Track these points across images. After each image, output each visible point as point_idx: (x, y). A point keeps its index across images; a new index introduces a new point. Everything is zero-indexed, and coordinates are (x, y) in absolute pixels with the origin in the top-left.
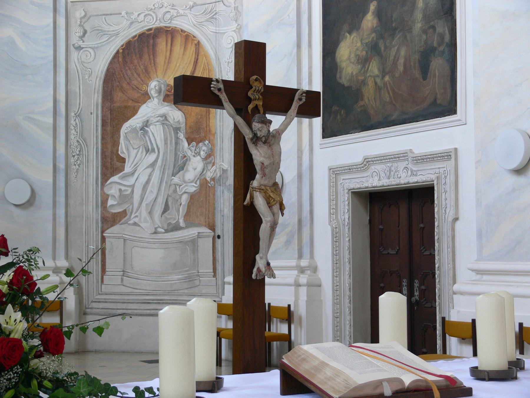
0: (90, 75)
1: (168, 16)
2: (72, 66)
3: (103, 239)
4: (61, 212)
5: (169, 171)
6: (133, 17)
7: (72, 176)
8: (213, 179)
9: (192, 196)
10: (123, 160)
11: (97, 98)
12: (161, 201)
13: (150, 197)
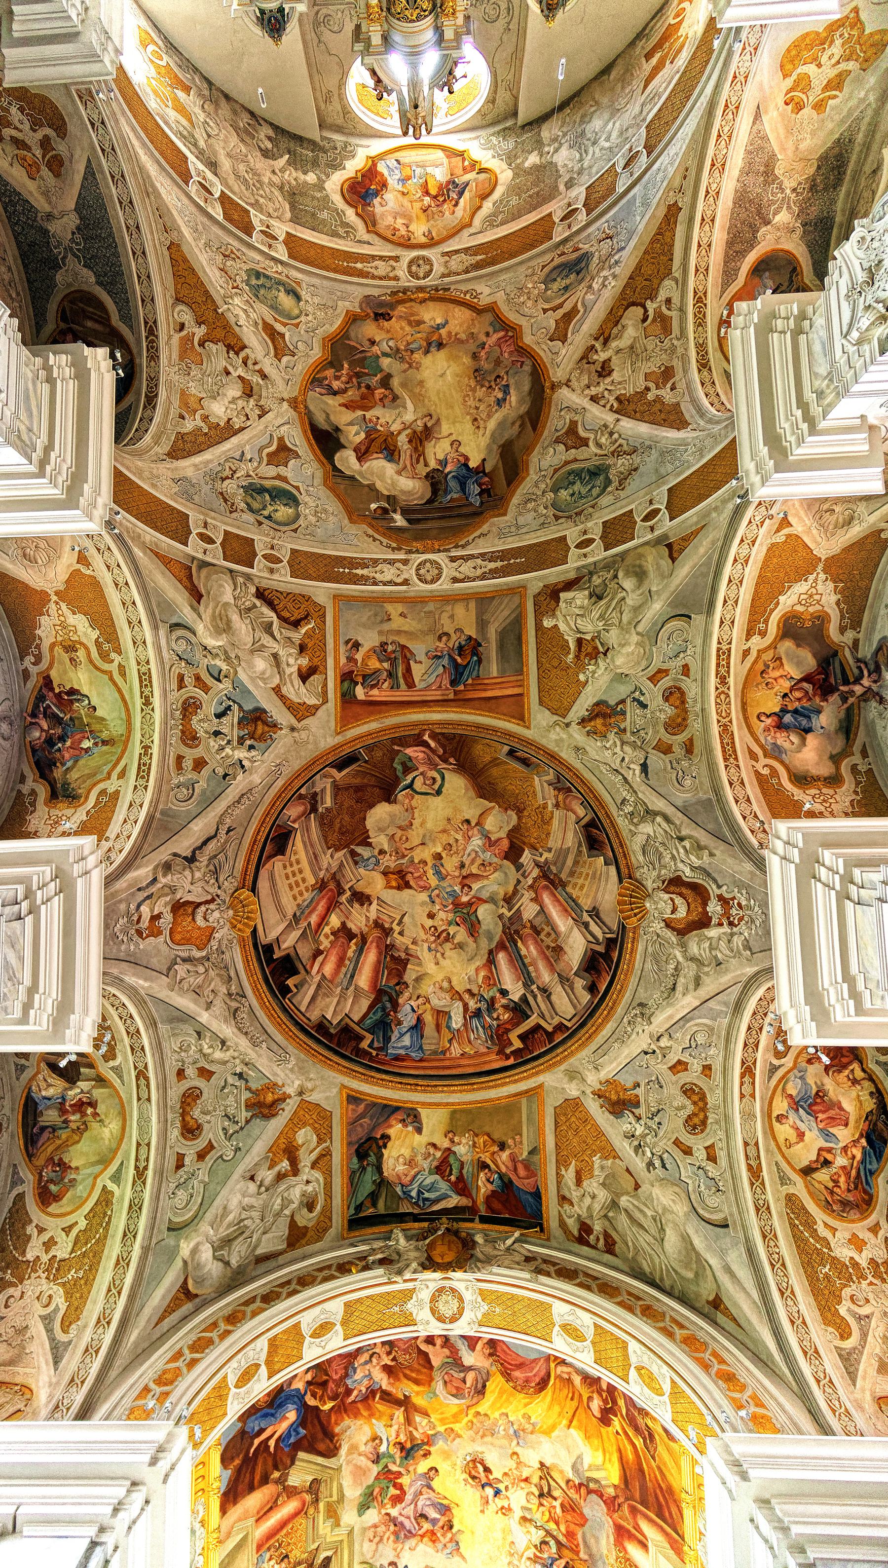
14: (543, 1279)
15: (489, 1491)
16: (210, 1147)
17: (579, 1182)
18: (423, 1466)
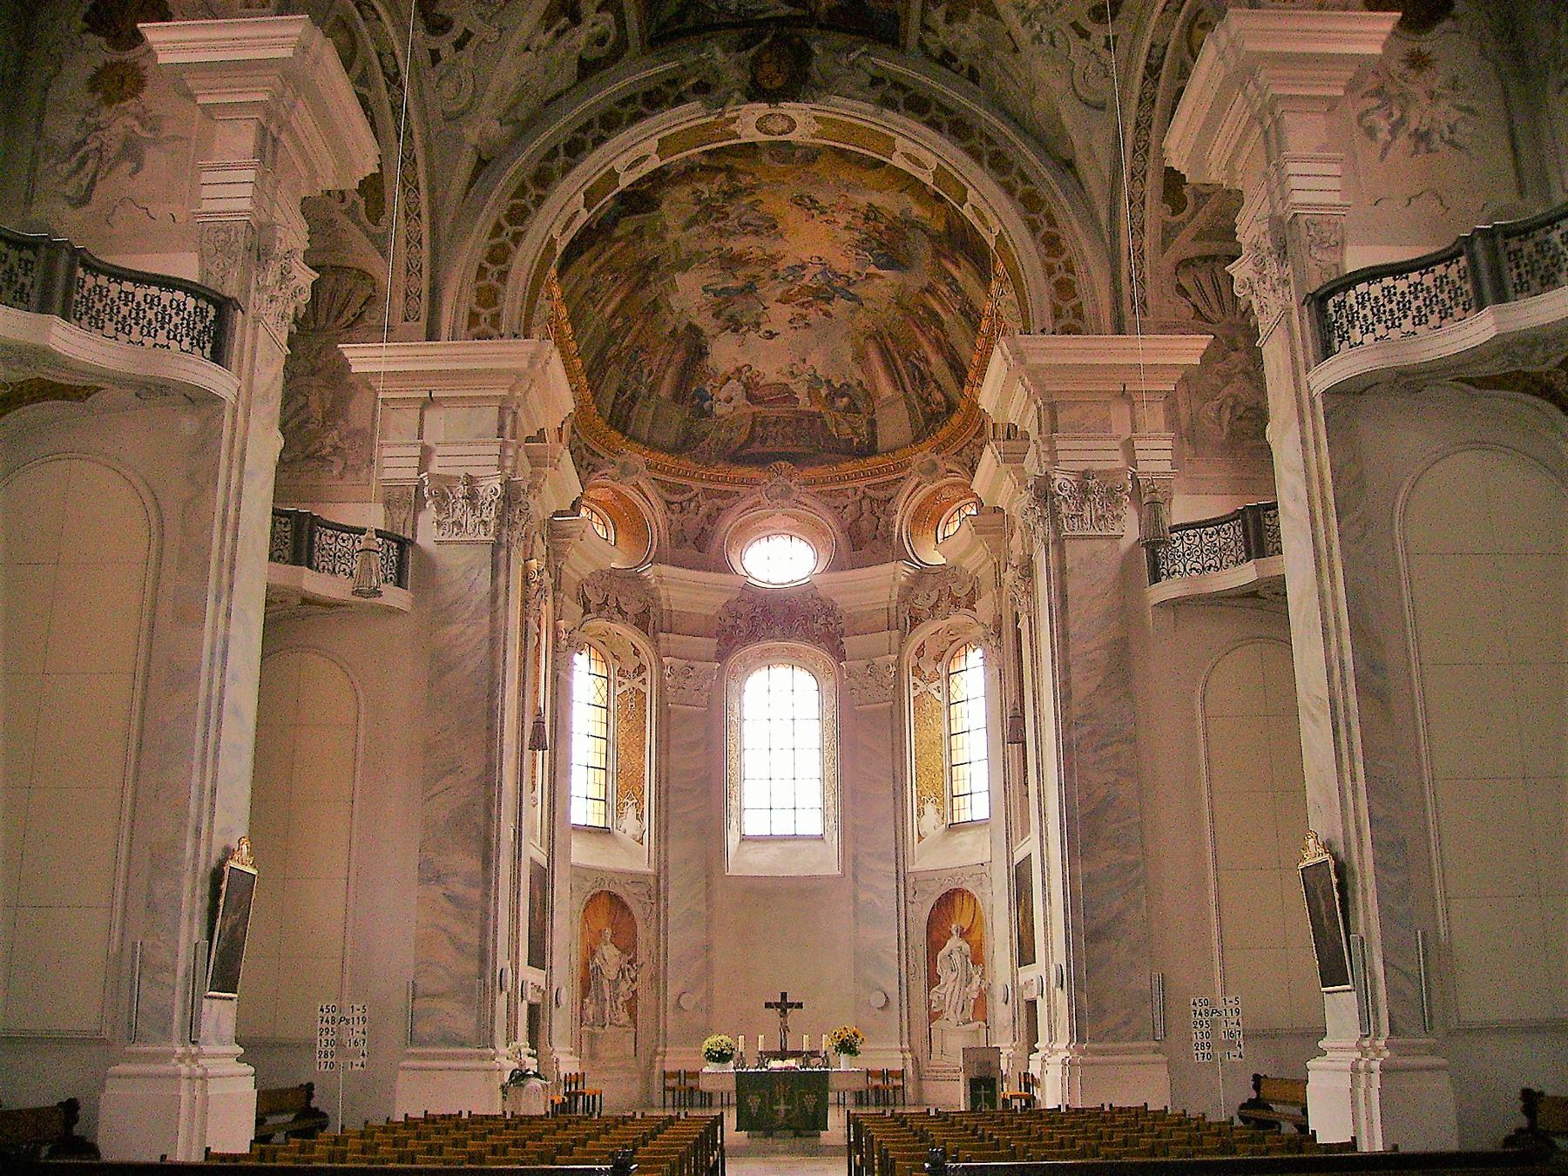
3: (930, 1029)
4: (905, 1011)
7: (911, 988)
13: (954, 1000)
14: (888, 113)
16: (468, 35)
17: (949, 19)
18: (746, 201)
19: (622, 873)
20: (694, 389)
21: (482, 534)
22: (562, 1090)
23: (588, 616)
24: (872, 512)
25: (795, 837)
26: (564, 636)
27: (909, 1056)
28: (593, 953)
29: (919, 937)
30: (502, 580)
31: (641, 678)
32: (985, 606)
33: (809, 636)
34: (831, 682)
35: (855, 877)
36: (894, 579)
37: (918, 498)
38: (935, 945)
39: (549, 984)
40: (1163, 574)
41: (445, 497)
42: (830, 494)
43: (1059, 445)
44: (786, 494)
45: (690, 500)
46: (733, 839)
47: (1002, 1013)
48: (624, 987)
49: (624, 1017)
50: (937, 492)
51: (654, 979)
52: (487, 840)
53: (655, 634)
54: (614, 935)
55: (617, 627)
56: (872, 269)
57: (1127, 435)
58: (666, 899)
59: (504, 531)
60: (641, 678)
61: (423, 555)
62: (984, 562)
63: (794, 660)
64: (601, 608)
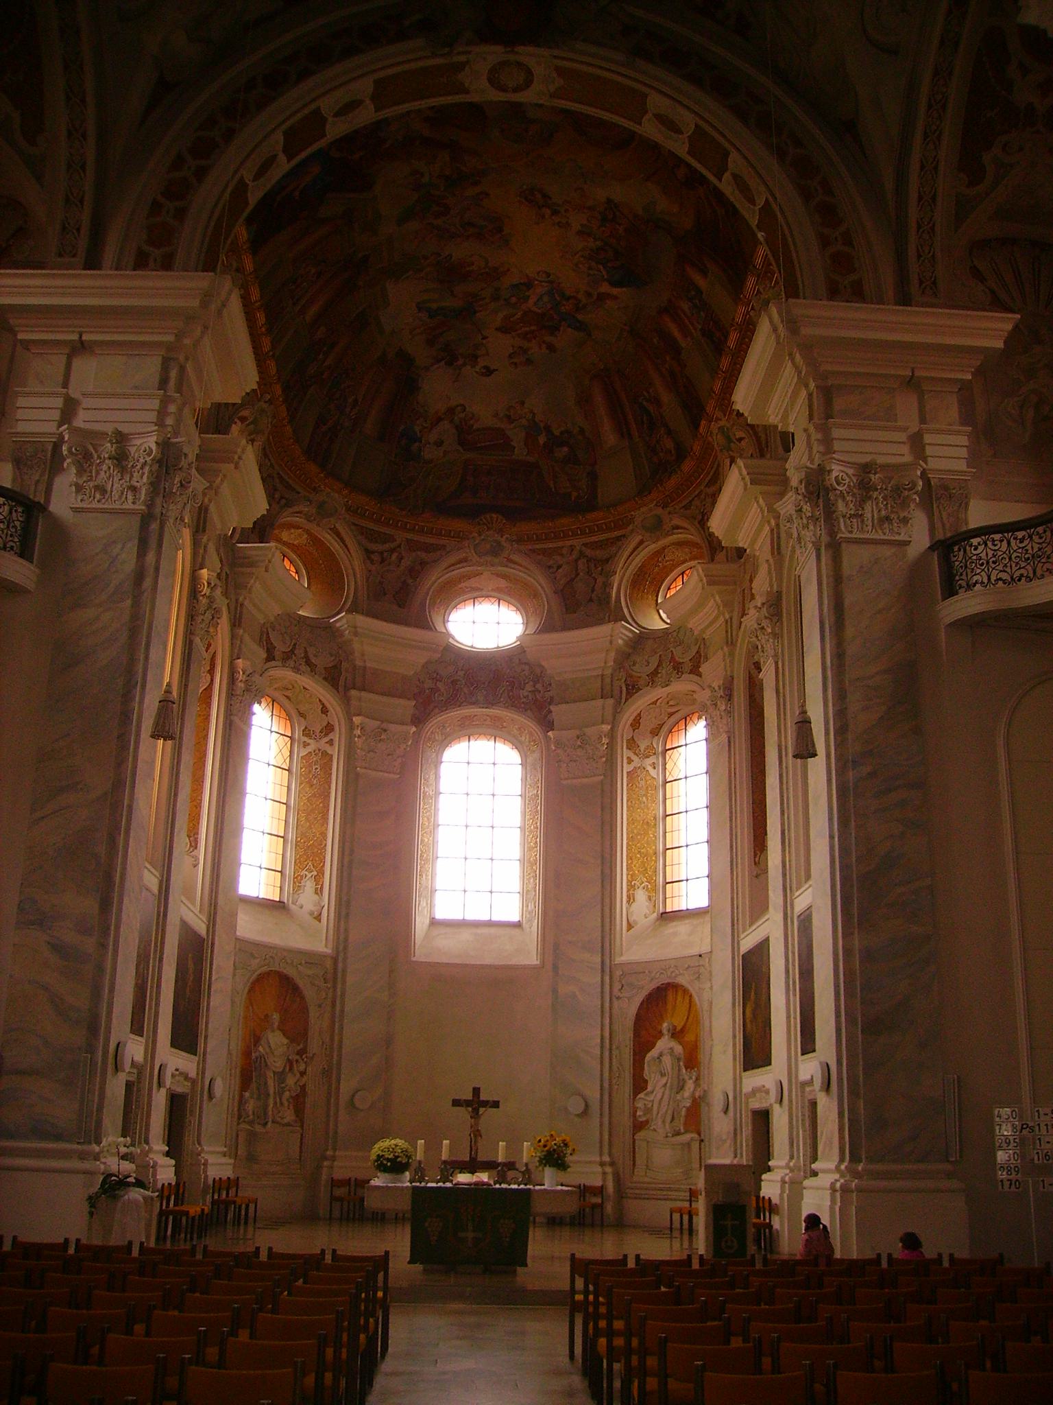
0: (626, 1018)
1: (673, 974)
2: (614, 1011)
4: (606, 1120)
5: (674, 1090)
6: (653, 975)
8: (699, 1097)
9: (688, 1109)
10: (646, 1082)
11: (630, 1034)
12: (670, 1112)
15: (548, 212)
19: (300, 952)
20: (402, 427)
21: (130, 501)
22: (209, 1198)
23: (273, 663)
24: (589, 573)
25: (490, 924)
26: (241, 676)
27: (609, 1169)
28: (257, 1040)
29: (625, 1037)
30: (151, 558)
31: (327, 739)
32: (713, 670)
33: (514, 703)
34: (537, 755)
35: (555, 968)
36: (611, 642)
37: (638, 560)
38: (642, 1045)
39: (202, 1071)
40: (961, 587)
41: (87, 456)
42: (544, 552)
43: (836, 433)
44: (496, 551)
45: (392, 551)
46: (420, 924)
47: (720, 1124)
48: (291, 1081)
49: (289, 1116)
50: (660, 553)
51: (327, 1073)
52: (109, 877)
53: (347, 689)
54: (283, 1022)
55: (304, 681)
56: (605, 288)
57: (914, 428)
58: (344, 982)
59: (159, 501)
60: (327, 739)
61: (57, 526)
62: (716, 619)
63: (496, 730)
64: (287, 656)
